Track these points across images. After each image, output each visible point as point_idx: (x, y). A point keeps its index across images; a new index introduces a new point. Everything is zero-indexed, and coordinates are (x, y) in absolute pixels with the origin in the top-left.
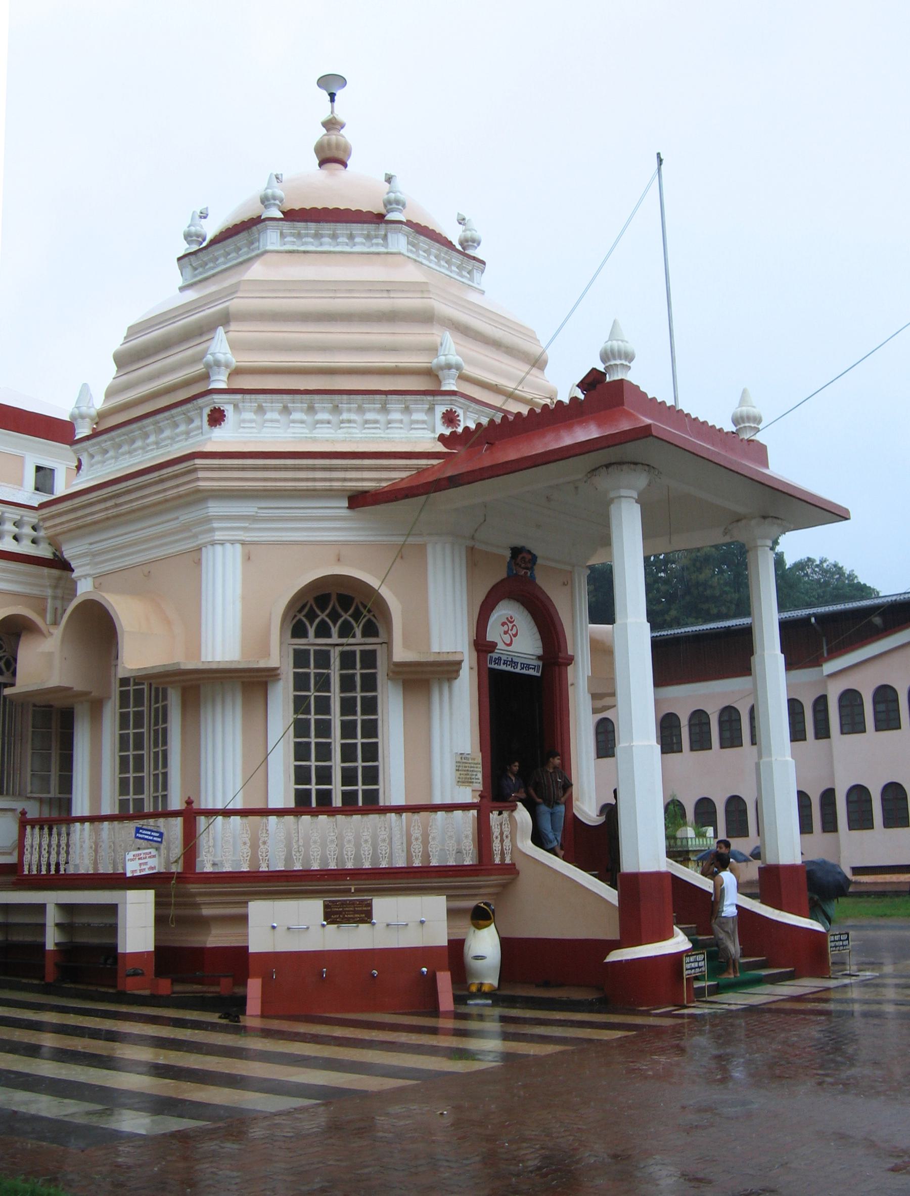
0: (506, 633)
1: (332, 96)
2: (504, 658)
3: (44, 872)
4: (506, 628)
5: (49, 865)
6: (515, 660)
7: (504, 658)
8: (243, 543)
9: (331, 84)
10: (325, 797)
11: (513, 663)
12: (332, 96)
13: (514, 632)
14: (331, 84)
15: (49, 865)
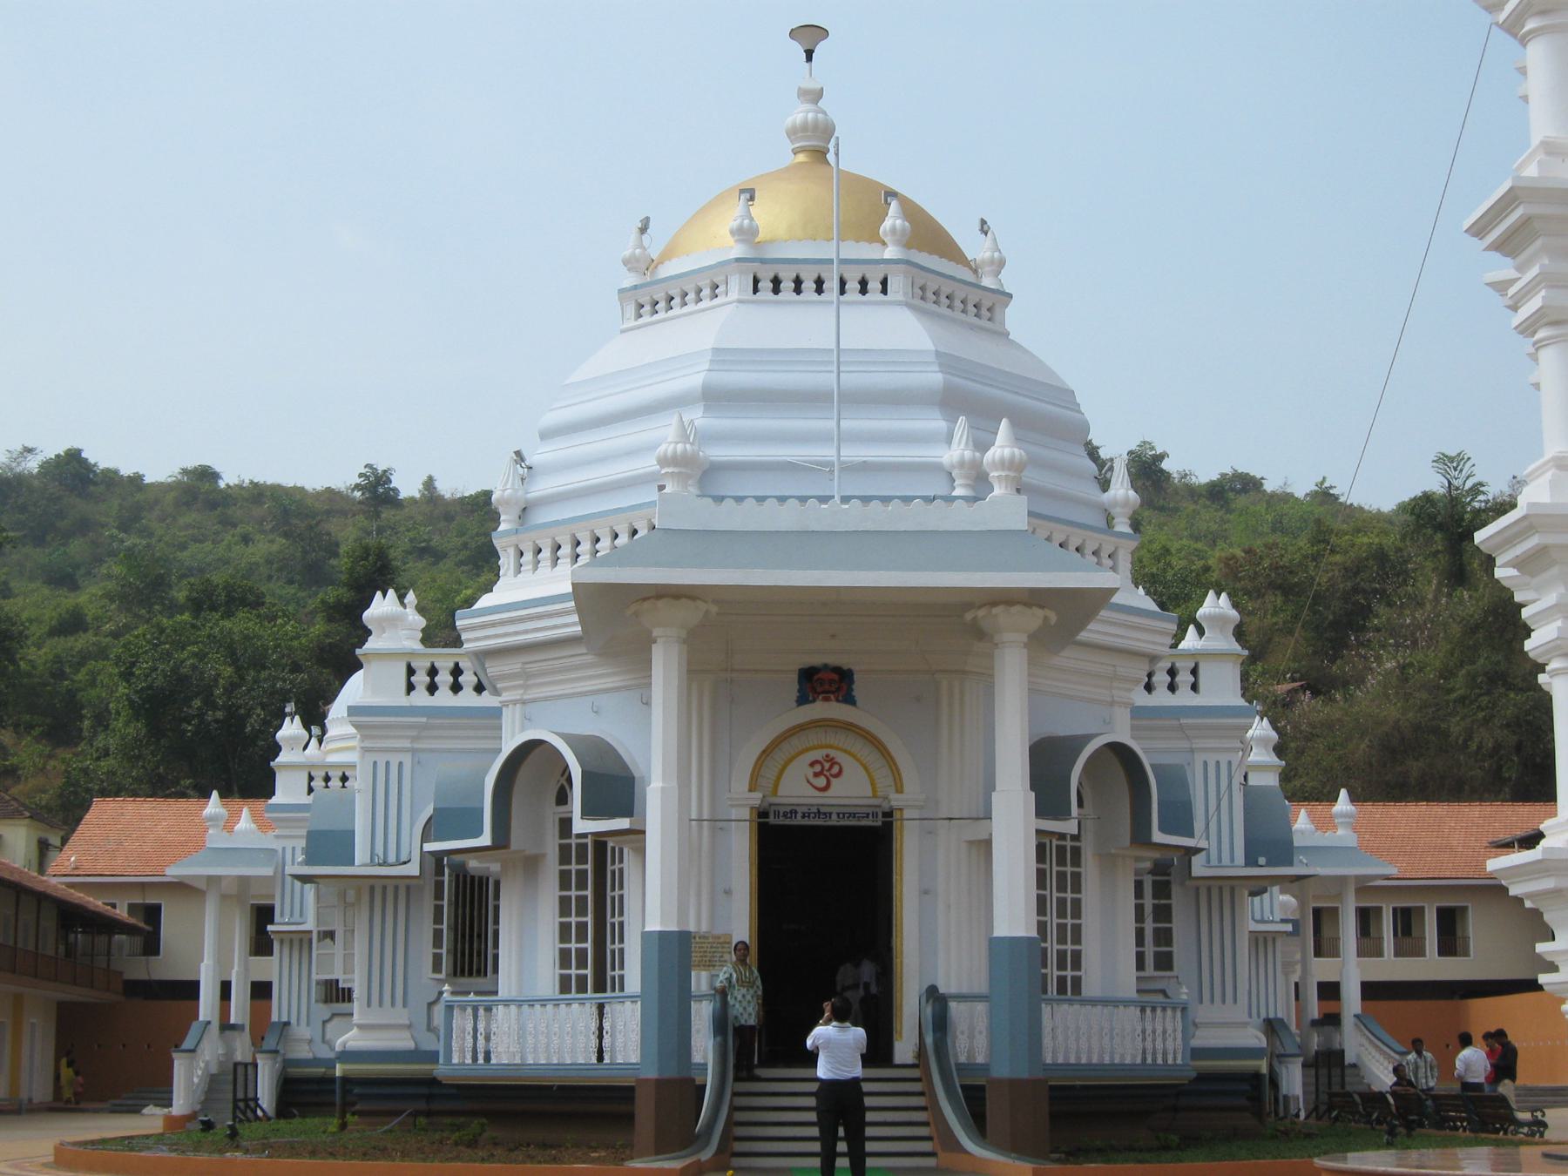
0: (816, 775)
1: (809, 55)
2: (800, 810)
3: (1160, 1061)
4: (818, 768)
5: (1154, 1054)
6: (823, 810)
7: (800, 810)
8: (524, 702)
9: (810, 37)
10: (582, 980)
11: (828, 815)
12: (809, 55)
13: (835, 769)
14: (810, 37)
15: (1154, 1054)
